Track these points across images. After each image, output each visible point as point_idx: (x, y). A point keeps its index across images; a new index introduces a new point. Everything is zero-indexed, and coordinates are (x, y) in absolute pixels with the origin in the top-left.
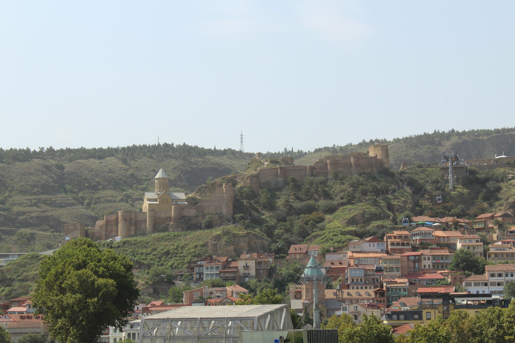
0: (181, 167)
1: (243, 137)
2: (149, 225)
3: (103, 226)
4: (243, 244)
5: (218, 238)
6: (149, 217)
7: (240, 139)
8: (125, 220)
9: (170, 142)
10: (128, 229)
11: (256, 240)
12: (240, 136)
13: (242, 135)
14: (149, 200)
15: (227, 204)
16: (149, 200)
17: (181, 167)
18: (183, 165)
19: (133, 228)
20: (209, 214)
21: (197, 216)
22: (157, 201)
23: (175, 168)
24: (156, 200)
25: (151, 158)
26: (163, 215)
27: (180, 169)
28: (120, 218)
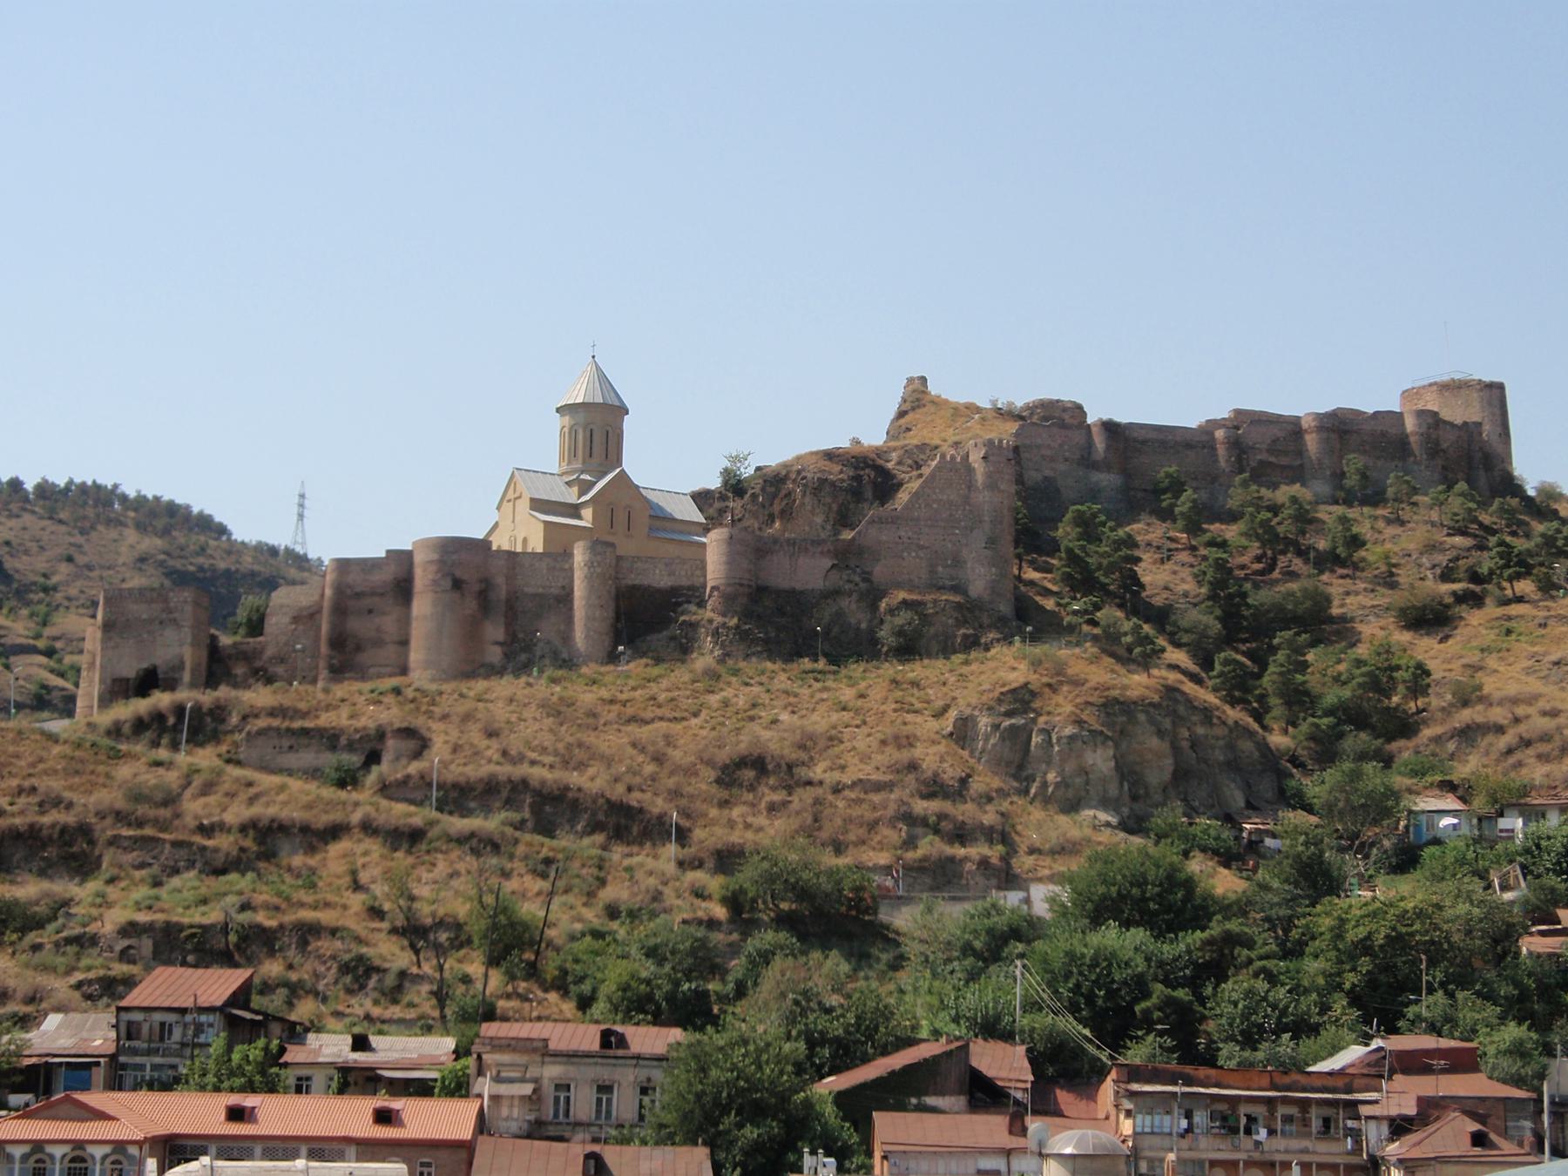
0: (162, 557)
1: (307, 503)
2: (589, 618)
3: (312, 616)
4: (1154, 742)
5: (1021, 700)
6: (589, 578)
7: (295, 509)
8: (457, 584)
9: (107, 481)
10: (471, 634)
11: (1200, 730)
12: (296, 500)
13: (302, 496)
14: (539, 505)
15: (992, 542)
16: (539, 505)
17: (162, 557)
18: (168, 554)
19: (494, 631)
20: (899, 586)
21: (835, 593)
22: (579, 517)
23: (142, 560)
24: (574, 510)
25: (51, 518)
26: (660, 579)
27: (161, 564)
28: (421, 579)
